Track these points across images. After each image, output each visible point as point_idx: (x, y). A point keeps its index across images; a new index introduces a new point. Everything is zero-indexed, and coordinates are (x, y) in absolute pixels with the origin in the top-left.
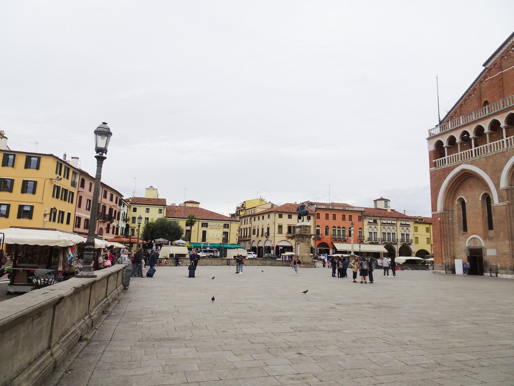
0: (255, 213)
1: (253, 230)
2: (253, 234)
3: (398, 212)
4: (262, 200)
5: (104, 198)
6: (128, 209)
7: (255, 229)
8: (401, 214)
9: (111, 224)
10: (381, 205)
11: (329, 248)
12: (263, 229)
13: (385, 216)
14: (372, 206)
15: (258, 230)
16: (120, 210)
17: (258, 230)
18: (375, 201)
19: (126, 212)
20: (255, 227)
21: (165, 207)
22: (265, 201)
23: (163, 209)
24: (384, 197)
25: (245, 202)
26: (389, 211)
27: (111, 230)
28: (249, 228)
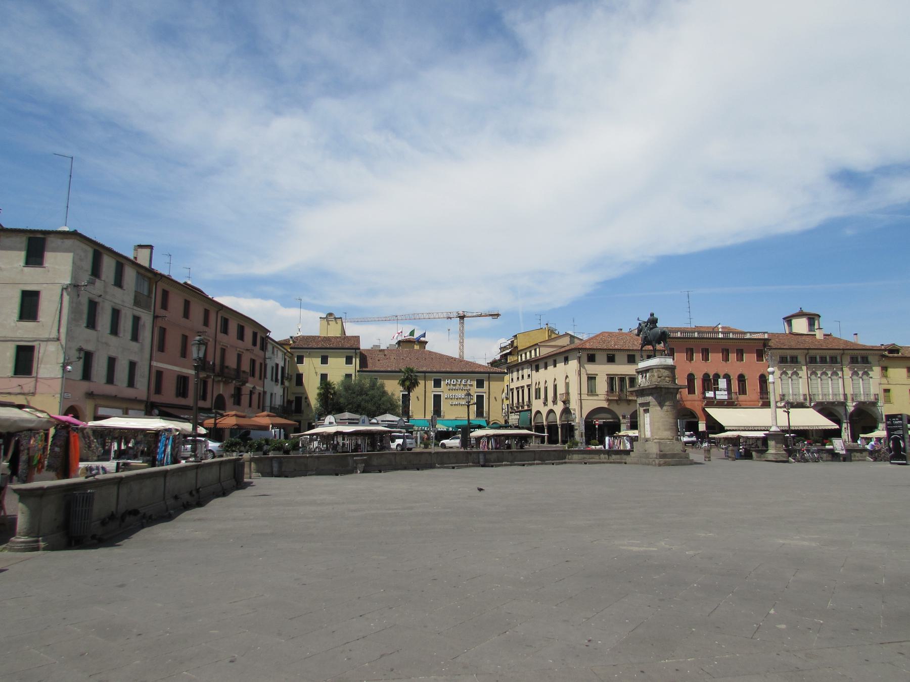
1: (536, 390)
2: (536, 398)
3: (841, 340)
4: (551, 331)
5: (221, 332)
6: (285, 359)
7: (540, 389)
8: (846, 342)
10: (800, 326)
11: (697, 420)
12: (555, 386)
13: (814, 347)
14: (781, 328)
15: (546, 388)
16: (265, 359)
17: (546, 388)
18: (788, 320)
19: (281, 364)
20: (539, 385)
22: (557, 332)
23: (354, 355)
24: (805, 310)
25: (515, 336)
26: (819, 335)
27: (245, 399)
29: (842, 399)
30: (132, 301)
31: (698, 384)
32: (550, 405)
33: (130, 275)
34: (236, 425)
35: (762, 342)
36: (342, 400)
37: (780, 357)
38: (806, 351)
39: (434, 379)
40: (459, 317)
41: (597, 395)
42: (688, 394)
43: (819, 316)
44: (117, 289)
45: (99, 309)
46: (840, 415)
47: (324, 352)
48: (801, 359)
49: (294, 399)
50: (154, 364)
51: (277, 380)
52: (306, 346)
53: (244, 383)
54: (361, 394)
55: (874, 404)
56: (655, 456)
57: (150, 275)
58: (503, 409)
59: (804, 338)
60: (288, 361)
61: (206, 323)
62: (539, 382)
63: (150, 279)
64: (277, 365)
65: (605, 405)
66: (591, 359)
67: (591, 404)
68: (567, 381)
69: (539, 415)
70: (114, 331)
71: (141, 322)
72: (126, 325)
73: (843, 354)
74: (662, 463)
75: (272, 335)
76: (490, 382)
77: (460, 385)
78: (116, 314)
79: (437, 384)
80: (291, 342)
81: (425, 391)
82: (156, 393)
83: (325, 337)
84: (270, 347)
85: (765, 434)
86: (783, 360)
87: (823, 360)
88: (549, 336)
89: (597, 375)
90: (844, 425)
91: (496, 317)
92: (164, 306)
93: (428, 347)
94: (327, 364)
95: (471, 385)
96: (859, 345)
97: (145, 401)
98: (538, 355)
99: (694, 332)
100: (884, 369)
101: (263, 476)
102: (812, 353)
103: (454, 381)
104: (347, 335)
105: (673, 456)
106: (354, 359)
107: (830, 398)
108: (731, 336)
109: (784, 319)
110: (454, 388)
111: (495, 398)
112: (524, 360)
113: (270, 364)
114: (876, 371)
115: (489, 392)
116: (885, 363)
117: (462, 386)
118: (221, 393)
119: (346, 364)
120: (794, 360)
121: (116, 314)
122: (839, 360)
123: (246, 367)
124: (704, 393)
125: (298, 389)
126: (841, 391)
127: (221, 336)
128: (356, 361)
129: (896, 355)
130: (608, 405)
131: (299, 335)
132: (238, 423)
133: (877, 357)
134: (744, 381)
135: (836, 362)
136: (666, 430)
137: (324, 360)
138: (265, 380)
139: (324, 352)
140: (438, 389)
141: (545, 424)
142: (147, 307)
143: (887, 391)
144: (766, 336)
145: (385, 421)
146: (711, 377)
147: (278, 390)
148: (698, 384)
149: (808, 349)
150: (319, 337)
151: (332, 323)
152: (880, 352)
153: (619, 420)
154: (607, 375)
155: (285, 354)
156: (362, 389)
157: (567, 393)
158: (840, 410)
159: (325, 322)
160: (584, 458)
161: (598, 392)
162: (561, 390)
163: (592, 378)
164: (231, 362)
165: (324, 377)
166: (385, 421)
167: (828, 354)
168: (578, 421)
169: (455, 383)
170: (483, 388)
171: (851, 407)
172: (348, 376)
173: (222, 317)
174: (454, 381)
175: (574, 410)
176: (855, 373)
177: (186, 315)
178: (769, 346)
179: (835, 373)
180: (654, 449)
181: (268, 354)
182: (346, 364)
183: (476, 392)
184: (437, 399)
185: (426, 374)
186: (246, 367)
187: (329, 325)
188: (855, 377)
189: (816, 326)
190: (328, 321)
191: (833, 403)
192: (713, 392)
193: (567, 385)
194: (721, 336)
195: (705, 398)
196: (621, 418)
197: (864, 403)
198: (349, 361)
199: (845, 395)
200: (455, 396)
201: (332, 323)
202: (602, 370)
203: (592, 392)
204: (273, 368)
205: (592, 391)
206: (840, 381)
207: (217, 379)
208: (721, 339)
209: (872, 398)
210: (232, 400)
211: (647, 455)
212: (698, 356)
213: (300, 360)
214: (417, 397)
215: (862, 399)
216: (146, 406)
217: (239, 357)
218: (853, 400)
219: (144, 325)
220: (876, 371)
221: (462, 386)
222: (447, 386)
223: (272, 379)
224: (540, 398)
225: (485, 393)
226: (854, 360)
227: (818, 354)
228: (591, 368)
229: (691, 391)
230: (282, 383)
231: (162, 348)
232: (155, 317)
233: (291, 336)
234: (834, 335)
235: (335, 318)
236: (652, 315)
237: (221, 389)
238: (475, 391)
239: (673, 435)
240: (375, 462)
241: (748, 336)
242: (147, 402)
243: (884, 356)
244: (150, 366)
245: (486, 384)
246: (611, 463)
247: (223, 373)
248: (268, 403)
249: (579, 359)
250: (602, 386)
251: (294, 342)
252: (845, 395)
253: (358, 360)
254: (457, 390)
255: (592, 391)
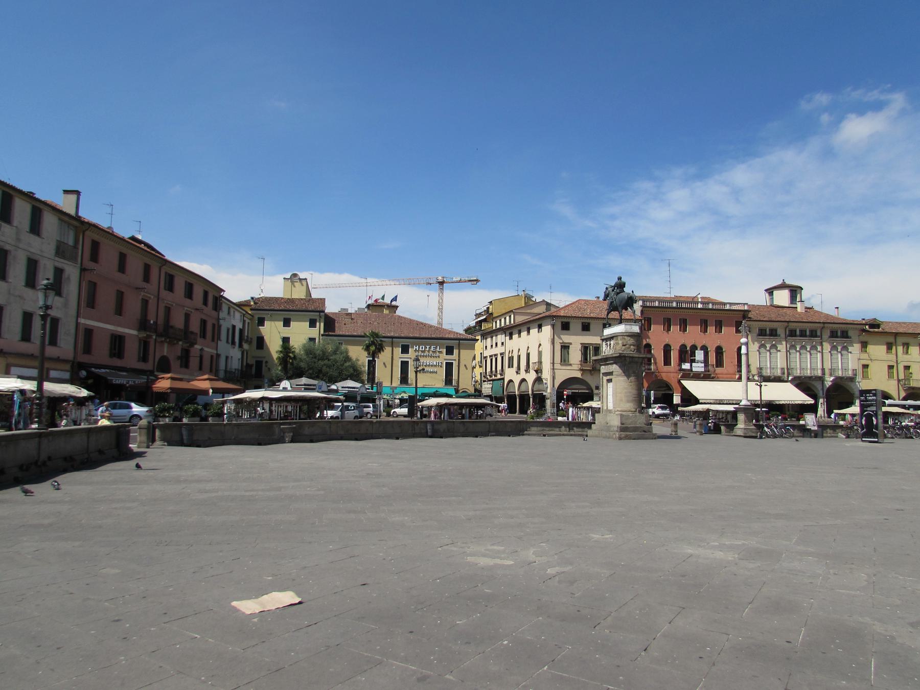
0: (512, 322)
1: (509, 358)
2: (509, 367)
3: (822, 313)
7: (513, 357)
8: (827, 316)
9: (192, 350)
10: (782, 298)
11: (671, 392)
12: (528, 355)
13: (794, 320)
15: (519, 357)
16: (218, 319)
17: (519, 357)
18: (770, 291)
19: (239, 326)
21: (321, 314)
22: (534, 299)
23: (318, 319)
24: (788, 282)
25: (491, 302)
27: (194, 362)
28: (501, 354)
29: (819, 373)
30: (53, 252)
31: (674, 355)
32: (523, 375)
33: (49, 222)
34: (170, 388)
35: (742, 313)
36: (303, 365)
37: (759, 330)
38: (786, 324)
39: (402, 345)
40: (439, 282)
41: (571, 365)
42: (664, 365)
43: (802, 289)
44: (33, 238)
45: (10, 258)
46: (817, 389)
47: (287, 315)
48: (781, 331)
49: (254, 363)
50: (82, 321)
51: (233, 343)
52: (268, 308)
53: (192, 344)
54: (322, 359)
55: (852, 379)
56: (616, 429)
57: (75, 223)
58: (472, 378)
59: (785, 310)
60: (248, 323)
61: (147, 278)
62: (512, 351)
63: (76, 227)
64: (234, 327)
65: (578, 375)
66: (566, 327)
67: (563, 374)
68: (540, 349)
69: (511, 383)
70: (31, 282)
71: (65, 275)
72: (44, 278)
73: (823, 328)
74: (623, 436)
75: (226, 295)
76: (461, 351)
77: (429, 351)
78: (32, 266)
79: (405, 350)
80: (252, 303)
81: (392, 357)
82: (84, 353)
83: (288, 299)
84: (225, 308)
85: (734, 408)
86: (762, 333)
87: (803, 334)
88: (525, 303)
89: (571, 344)
90: (821, 401)
91: (475, 283)
92: (95, 257)
93: (399, 312)
94: (289, 326)
95: (440, 352)
96: (839, 319)
97: (71, 361)
98: (512, 322)
99: (672, 302)
100: (864, 345)
101: (169, 445)
102: (792, 326)
103: (422, 347)
104: (312, 297)
105: (635, 429)
106: (318, 324)
107: (808, 373)
108: (710, 306)
109: (766, 290)
110: (422, 354)
111: (465, 366)
112: (498, 327)
113: (225, 325)
114: (856, 348)
115: (459, 360)
116: (865, 337)
117: (431, 352)
118: (165, 354)
119: (310, 327)
120: (773, 333)
121: (32, 266)
122: (819, 334)
123: (195, 327)
124: (680, 365)
125: (259, 353)
126: (819, 366)
127: (164, 293)
128: (321, 326)
129: (876, 330)
130: (582, 375)
131: (262, 295)
132: (172, 387)
133: (857, 332)
134: (722, 353)
135: (816, 336)
136: (628, 401)
137: (287, 323)
138: (219, 342)
139: (287, 315)
140: (405, 355)
141: (517, 393)
142: (73, 259)
143: (865, 366)
144: (746, 308)
145: (346, 387)
146: (688, 349)
147: (235, 354)
148: (674, 355)
149: (788, 322)
150: (282, 298)
151: (297, 284)
152: (859, 327)
153: (592, 391)
154: (581, 344)
155: (244, 315)
156: (324, 352)
157: (540, 362)
158: (818, 385)
159: (289, 283)
160: (543, 430)
161: (571, 362)
162: (534, 359)
163: (565, 347)
164: (178, 321)
165: (286, 340)
166: (346, 387)
167: (808, 327)
168: (549, 391)
169: (423, 350)
170: (453, 355)
171: (829, 381)
172: (312, 340)
173: (166, 273)
174: (422, 348)
175: (547, 380)
176: (834, 348)
177: (122, 268)
178: (750, 318)
179: (814, 348)
180: (615, 422)
181: (222, 315)
182: (310, 327)
183: (445, 360)
184: (405, 365)
185: (394, 339)
186: (195, 327)
187: (294, 286)
188: (834, 352)
189: (798, 299)
190: (293, 282)
191: (810, 378)
192: (689, 364)
193: (540, 353)
194: (700, 306)
195: (681, 370)
196: (594, 388)
197: (841, 378)
198: (312, 324)
199: (823, 370)
200: (423, 362)
201: (297, 284)
202: (576, 341)
203: (565, 361)
204: (228, 330)
205: (565, 361)
206: (819, 355)
207: (159, 339)
208: (700, 309)
209: (850, 374)
210: (179, 362)
211: (607, 427)
212: (675, 329)
213: (261, 322)
214: (384, 364)
215: (840, 373)
216: (72, 367)
217: (187, 316)
218: (831, 375)
219: (69, 278)
220: (856, 348)
221: (431, 352)
222: (416, 352)
223: (227, 342)
224: (512, 367)
225: (455, 360)
226: (833, 335)
227: (798, 327)
228: (567, 338)
229: (667, 362)
230: (241, 346)
231: (91, 302)
232: (83, 270)
233: (252, 296)
234: (816, 308)
235: (300, 279)
236: (620, 278)
237: (165, 350)
238: (444, 358)
239: (636, 407)
240: (307, 431)
241: (728, 307)
242: (73, 362)
243: (864, 331)
244: (77, 324)
245: (456, 351)
246: (571, 435)
247: (167, 332)
248: (222, 366)
249: (553, 326)
250: (575, 356)
251: (255, 303)
252: (823, 370)
253: (322, 324)
254: (426, 356)
255: (565, 361)
